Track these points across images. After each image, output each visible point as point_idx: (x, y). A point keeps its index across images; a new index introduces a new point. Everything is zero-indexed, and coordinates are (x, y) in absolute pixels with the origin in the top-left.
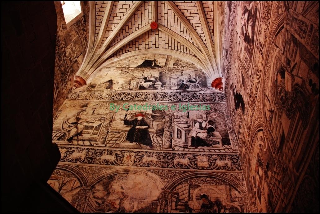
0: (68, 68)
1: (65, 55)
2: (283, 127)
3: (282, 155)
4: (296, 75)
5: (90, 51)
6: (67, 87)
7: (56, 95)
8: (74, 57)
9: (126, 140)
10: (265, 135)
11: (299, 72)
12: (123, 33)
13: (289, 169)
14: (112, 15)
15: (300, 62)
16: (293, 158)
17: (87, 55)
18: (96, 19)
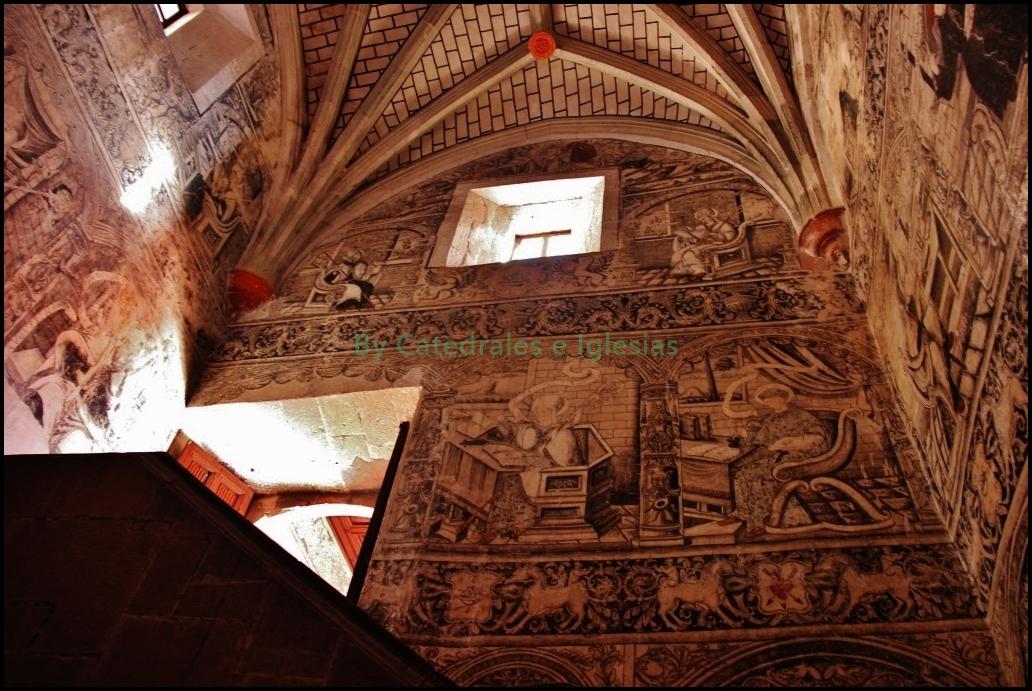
0: (747, 275)
1: (693, 282)
5: (748, 159)
6: (816, 298)
7: (812, 359)
8: (729, 236)
9: (1001, 116)
12: (706, 16)
14: (641, 55)
17: (757, 174)
18: (651, 117)
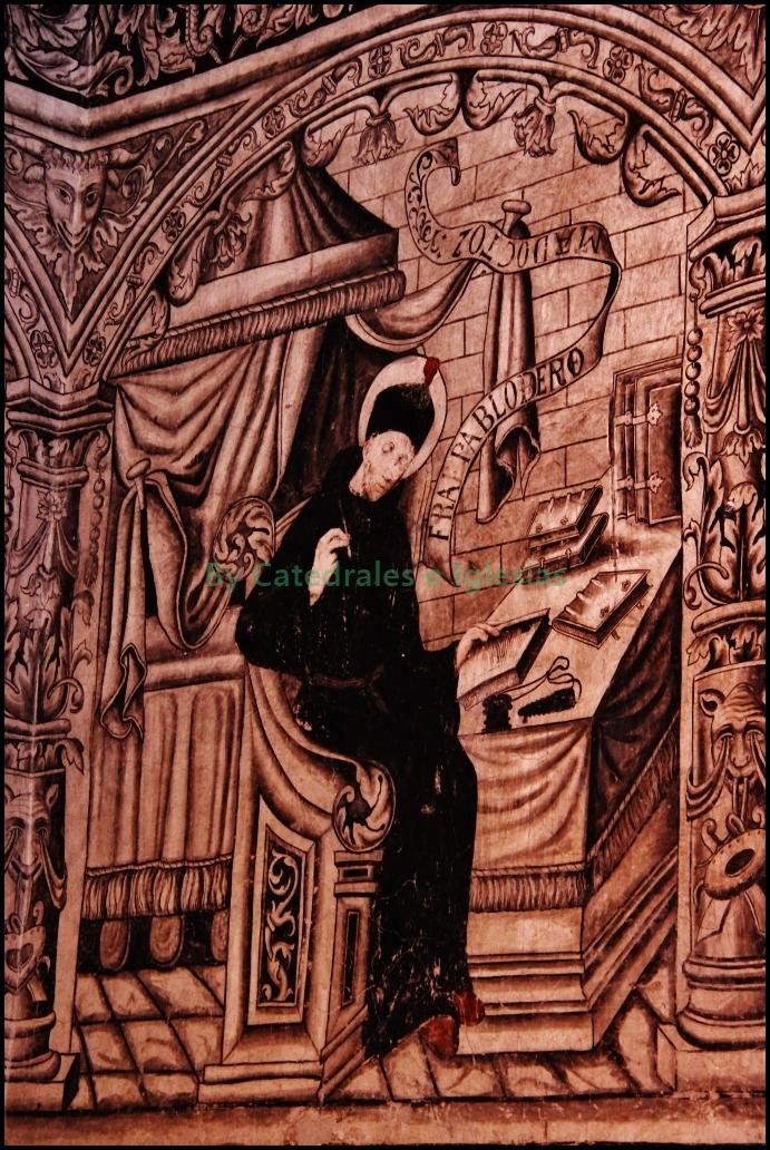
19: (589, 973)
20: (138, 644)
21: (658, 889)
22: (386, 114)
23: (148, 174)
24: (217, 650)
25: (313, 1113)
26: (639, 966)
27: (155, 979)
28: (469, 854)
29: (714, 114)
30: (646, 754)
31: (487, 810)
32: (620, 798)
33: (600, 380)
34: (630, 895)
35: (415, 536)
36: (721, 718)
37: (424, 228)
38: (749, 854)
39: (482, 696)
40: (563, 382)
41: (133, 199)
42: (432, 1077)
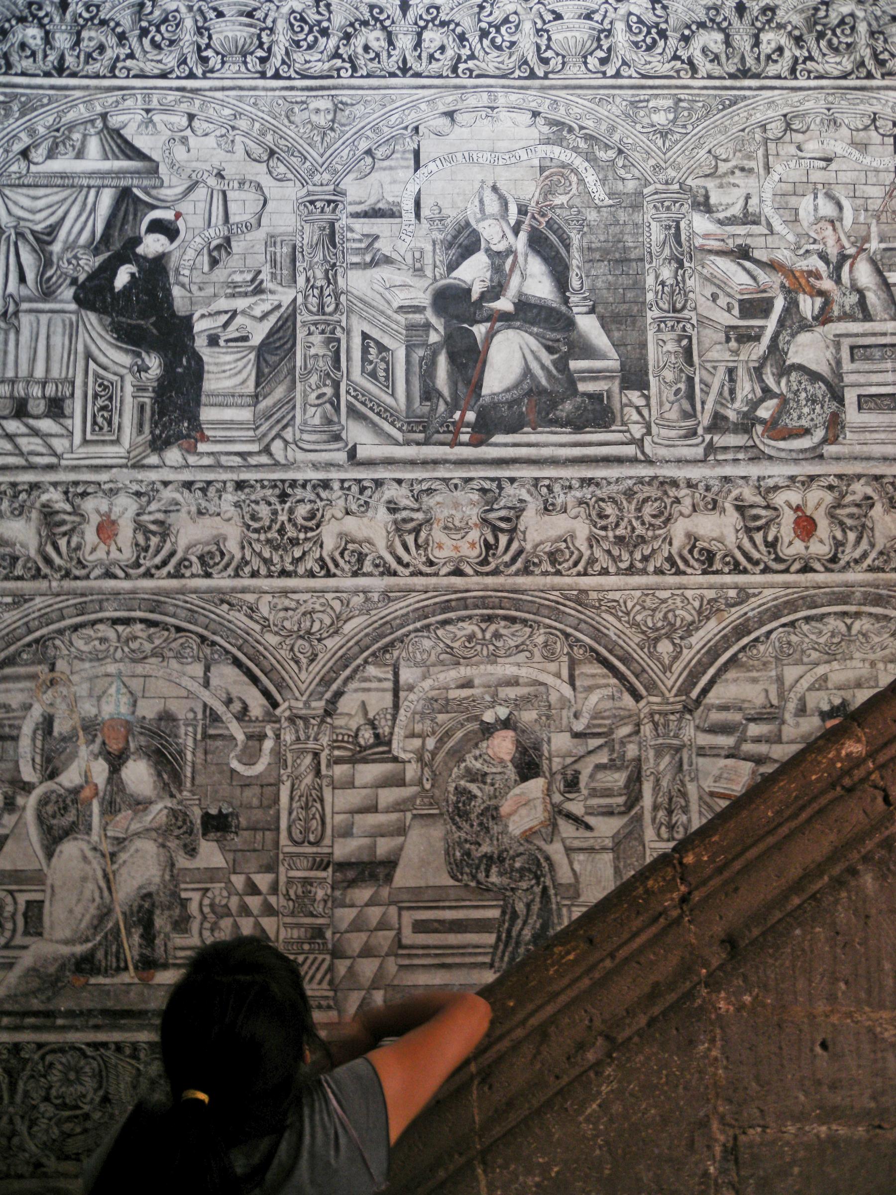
2: (401, 848)
3: (338, 893)
4: (568, 842)
10: (278, 737)
11: (582, 857)
13: (348, 962)
15: (604, 849)
16: (391, 965)
19: (257, 428)
20: (15, 293)
21: (288, 402)
22: (151, 121)
23: (15, 108)
24: (61, 301)
25: (125, 470)
26: (280, 426)
27: (31, 422)
28: (200, 388)
29: (306, 158)
30: (282, 360)
31: (208, 372)
32: (270, 373)
33: (259, 235)
34: (275, 405)
35: (172, 274)
36: (313, 351)
37: (173, 165)
38: (325, 394)
39: (207, 333)
40: (243, 232)
41: (7, 116)
42: (185, 459)
